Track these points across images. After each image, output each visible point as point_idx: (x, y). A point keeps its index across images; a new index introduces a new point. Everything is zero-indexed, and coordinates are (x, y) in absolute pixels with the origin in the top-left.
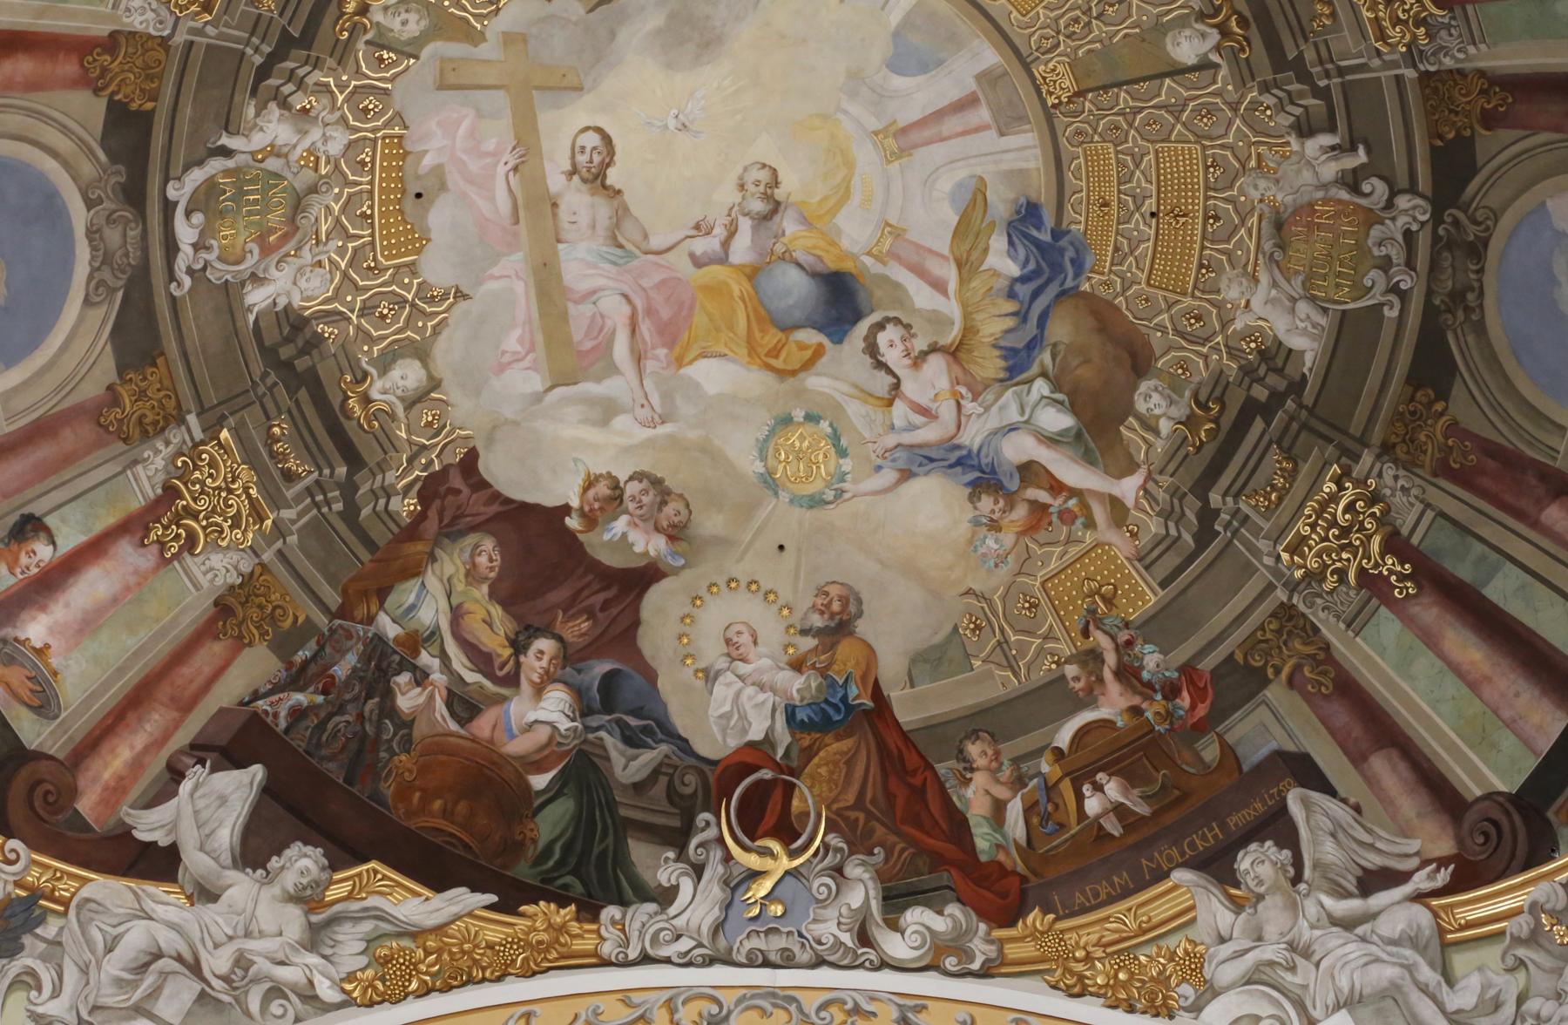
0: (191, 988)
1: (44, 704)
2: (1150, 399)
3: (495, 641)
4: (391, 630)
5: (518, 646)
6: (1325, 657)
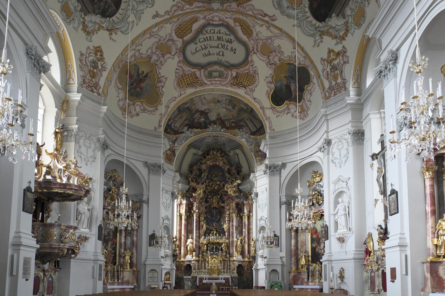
0: (185, 138)
1: (176, 128)
2: (236, 107)
3: (200, 117)
4: (194, 117)
5: (201, 117)
6: (245, 121)
